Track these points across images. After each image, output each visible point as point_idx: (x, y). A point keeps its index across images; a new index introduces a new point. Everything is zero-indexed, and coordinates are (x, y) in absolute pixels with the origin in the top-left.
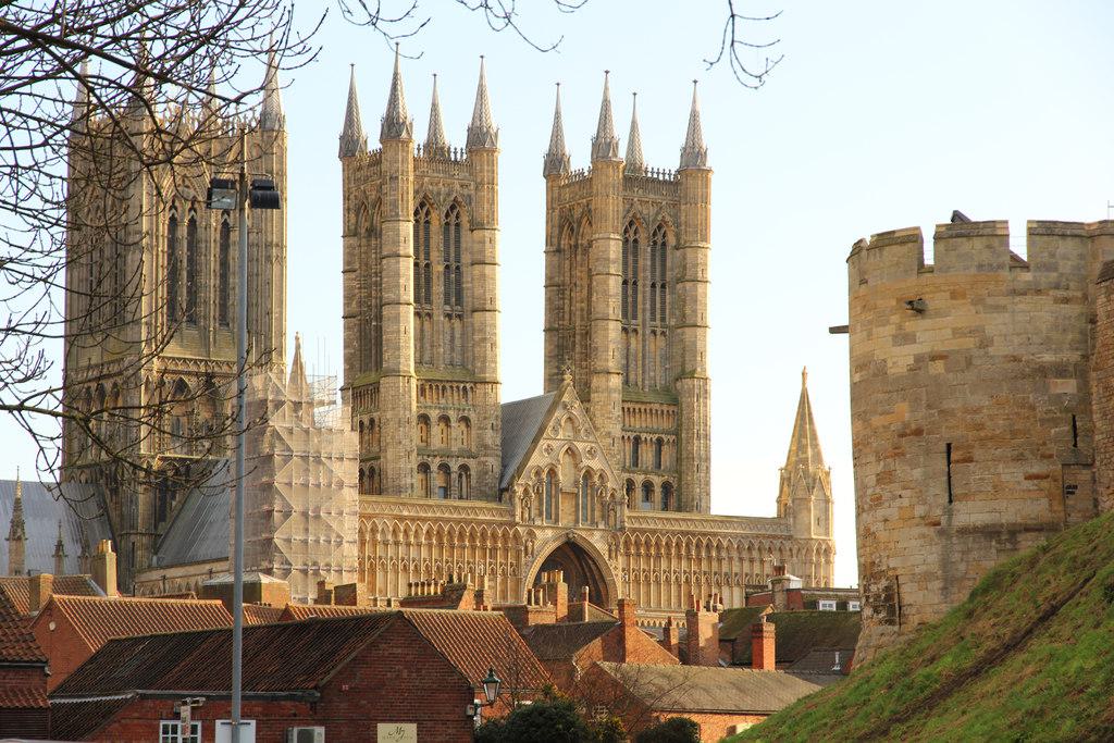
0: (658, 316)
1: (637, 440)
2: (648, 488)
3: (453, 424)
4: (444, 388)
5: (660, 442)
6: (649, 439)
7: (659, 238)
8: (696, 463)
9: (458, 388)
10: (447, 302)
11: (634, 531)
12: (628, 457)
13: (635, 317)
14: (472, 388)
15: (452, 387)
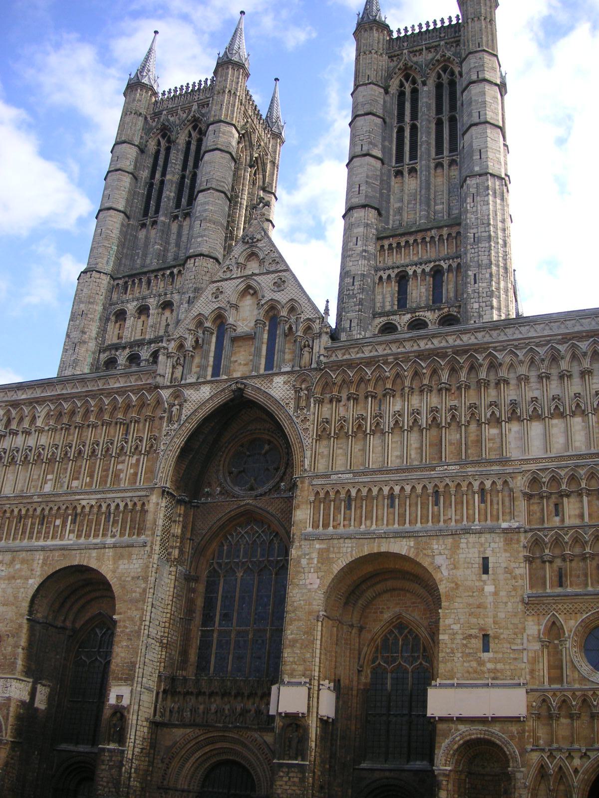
0: (446, 145)
1: (403, 279)
2: (418, 324)
3: (151, 311)
4: (149, 282)
5: (437, 273)
6: (419, 271)
7: (445, 78)
8: (470, 273)
9: (163, 275)
10: (178, 205)
11: (338, 366)
12: (389, 299)
13: (413, 156)
14: (180, 272)
15: (156, 276)
